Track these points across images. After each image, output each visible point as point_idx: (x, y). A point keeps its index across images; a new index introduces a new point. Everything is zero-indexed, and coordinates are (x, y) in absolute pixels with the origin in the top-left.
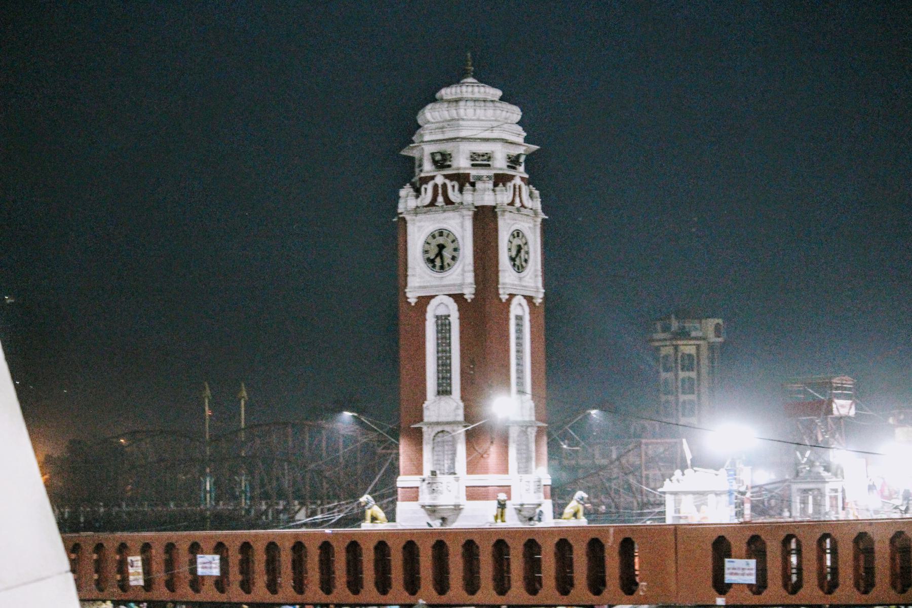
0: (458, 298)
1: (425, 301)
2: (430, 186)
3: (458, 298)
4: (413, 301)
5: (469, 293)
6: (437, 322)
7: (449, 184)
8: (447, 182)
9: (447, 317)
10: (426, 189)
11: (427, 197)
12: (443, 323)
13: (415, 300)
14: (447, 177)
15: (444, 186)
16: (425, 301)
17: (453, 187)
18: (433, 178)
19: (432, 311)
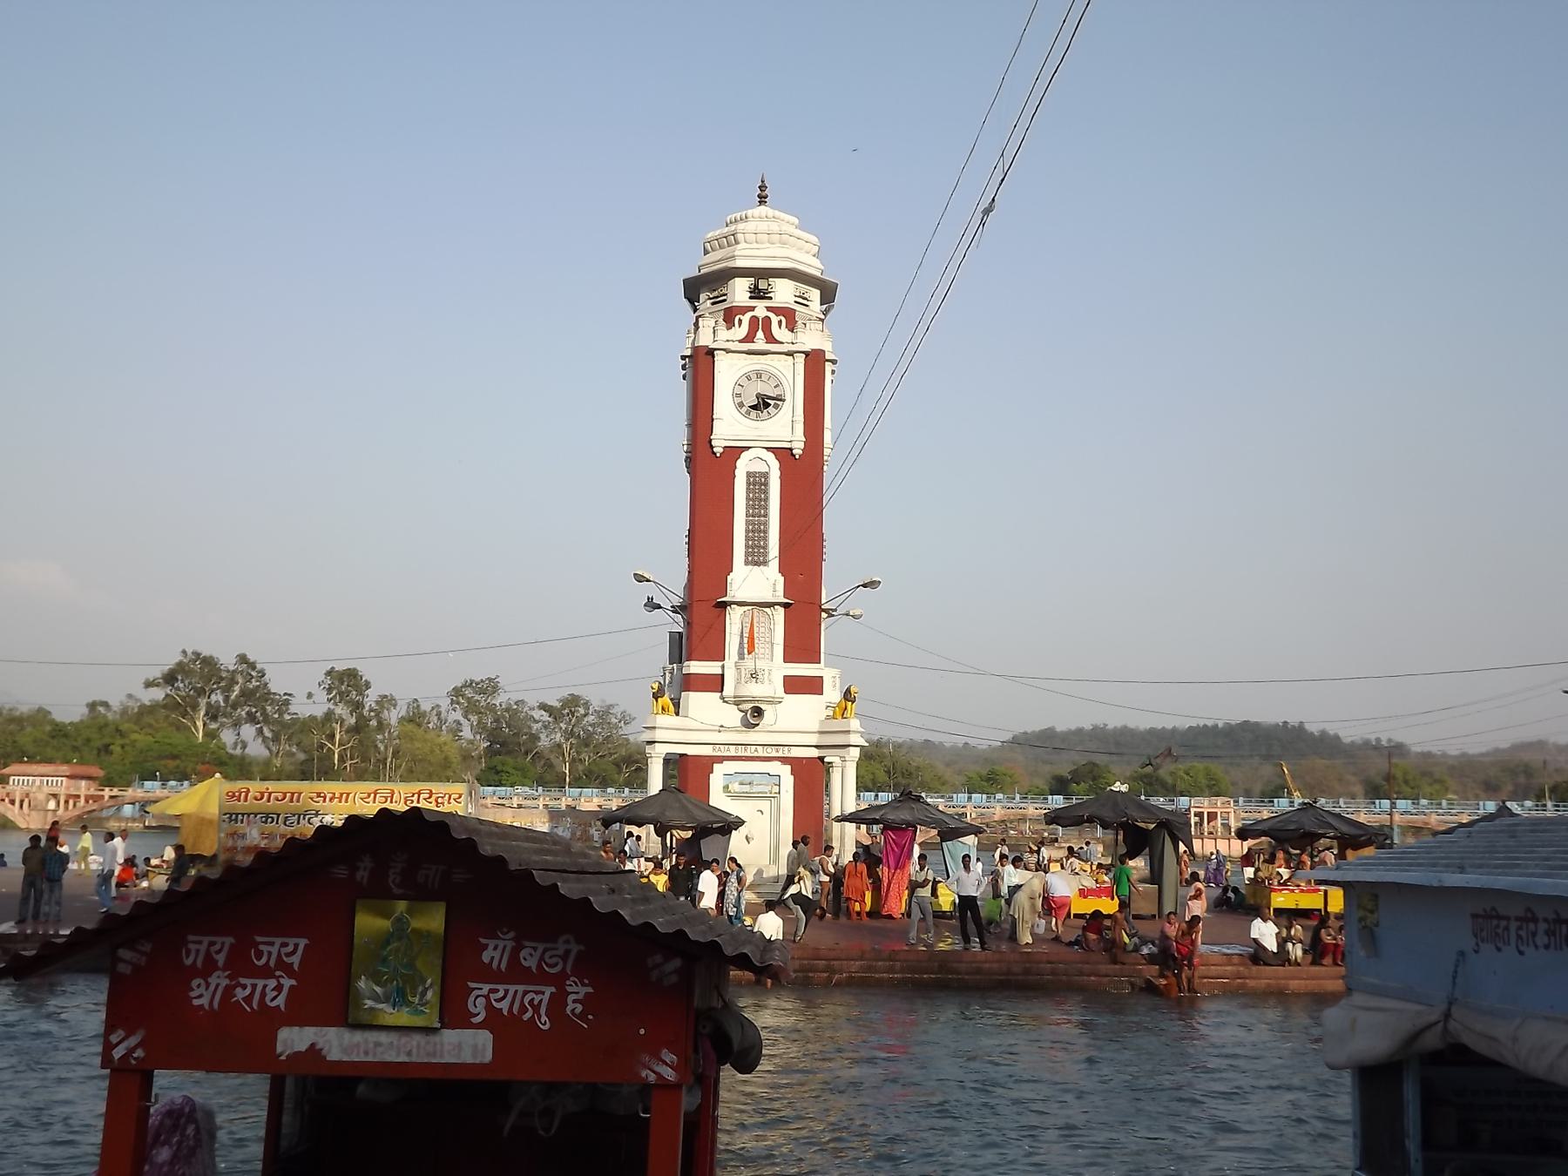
0: (783, 454)
1: (734, 452)
2: (746, 318)
3: (783, 454)
4: (718, 450)
5: (798, 448)
6: (748, 480)
7: (775, 319)
8: (771, 315)
9: (766, 475)
10: (740, 321)
11: (742, 331)
12: (758, 483)
13: (722, 450)
14: (769, 309)
15: (767, 320)
16: (734, 452)
17: (780, 322)
18: (752, 309)
19: (743, 466)
